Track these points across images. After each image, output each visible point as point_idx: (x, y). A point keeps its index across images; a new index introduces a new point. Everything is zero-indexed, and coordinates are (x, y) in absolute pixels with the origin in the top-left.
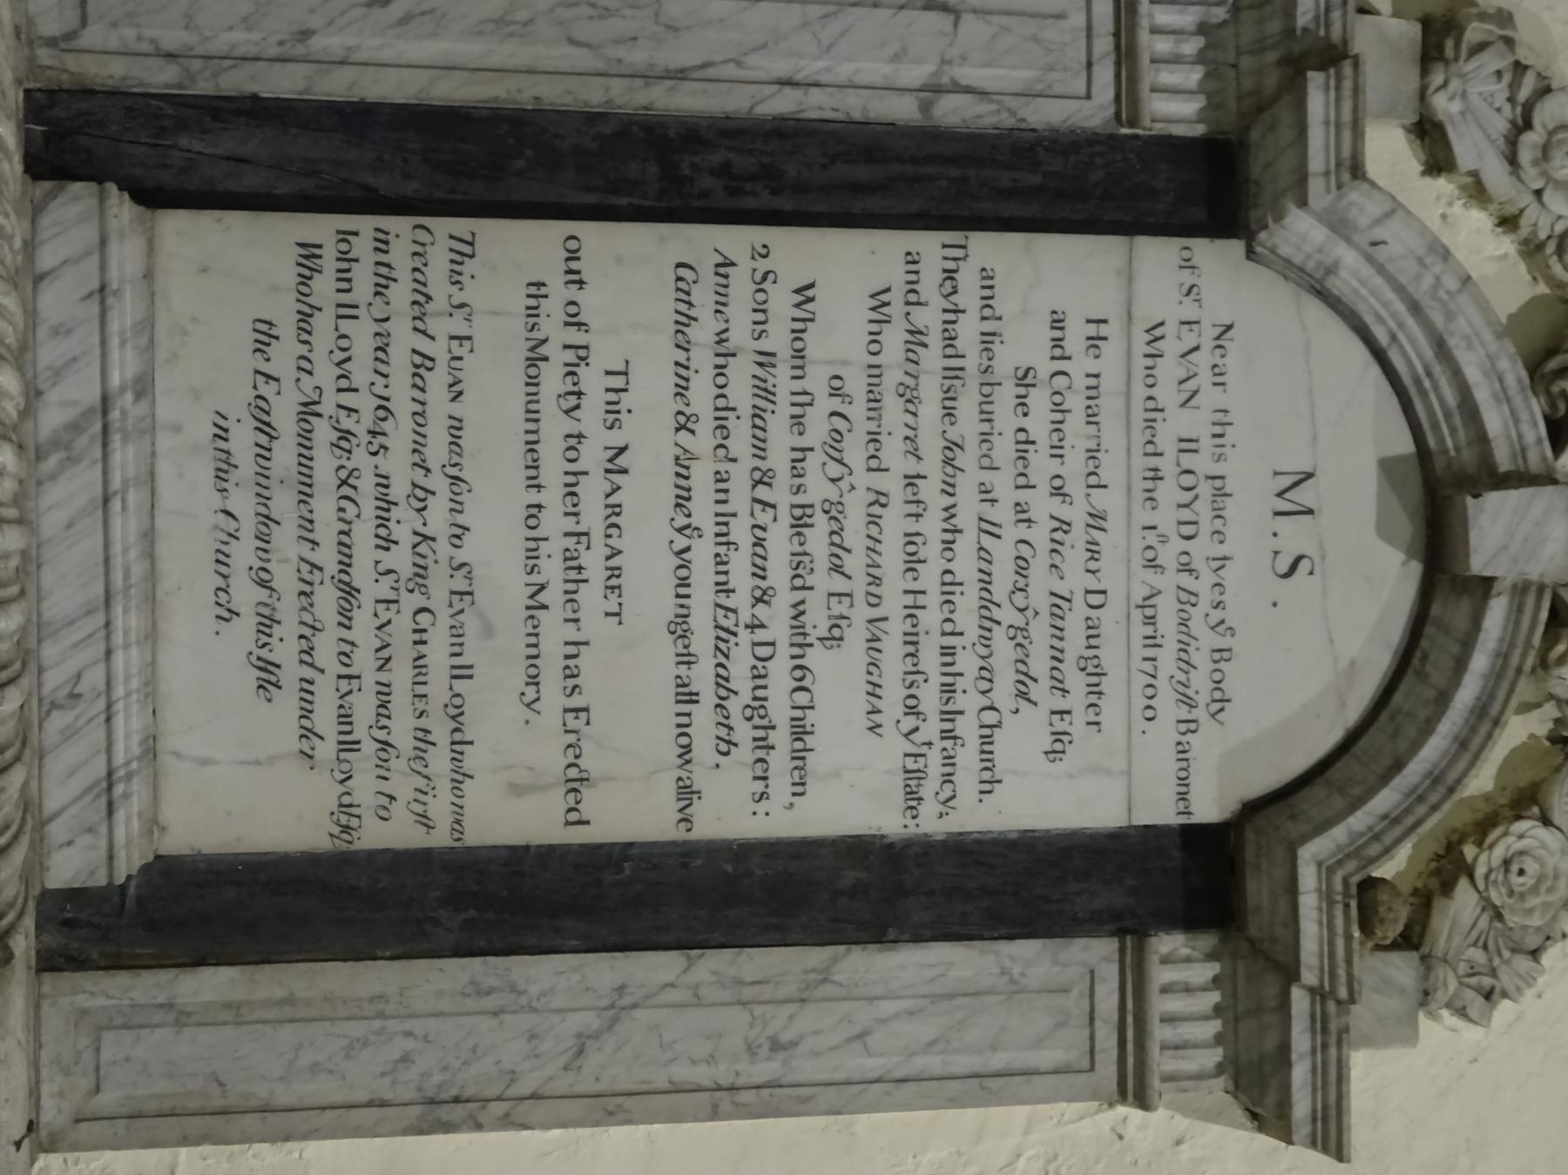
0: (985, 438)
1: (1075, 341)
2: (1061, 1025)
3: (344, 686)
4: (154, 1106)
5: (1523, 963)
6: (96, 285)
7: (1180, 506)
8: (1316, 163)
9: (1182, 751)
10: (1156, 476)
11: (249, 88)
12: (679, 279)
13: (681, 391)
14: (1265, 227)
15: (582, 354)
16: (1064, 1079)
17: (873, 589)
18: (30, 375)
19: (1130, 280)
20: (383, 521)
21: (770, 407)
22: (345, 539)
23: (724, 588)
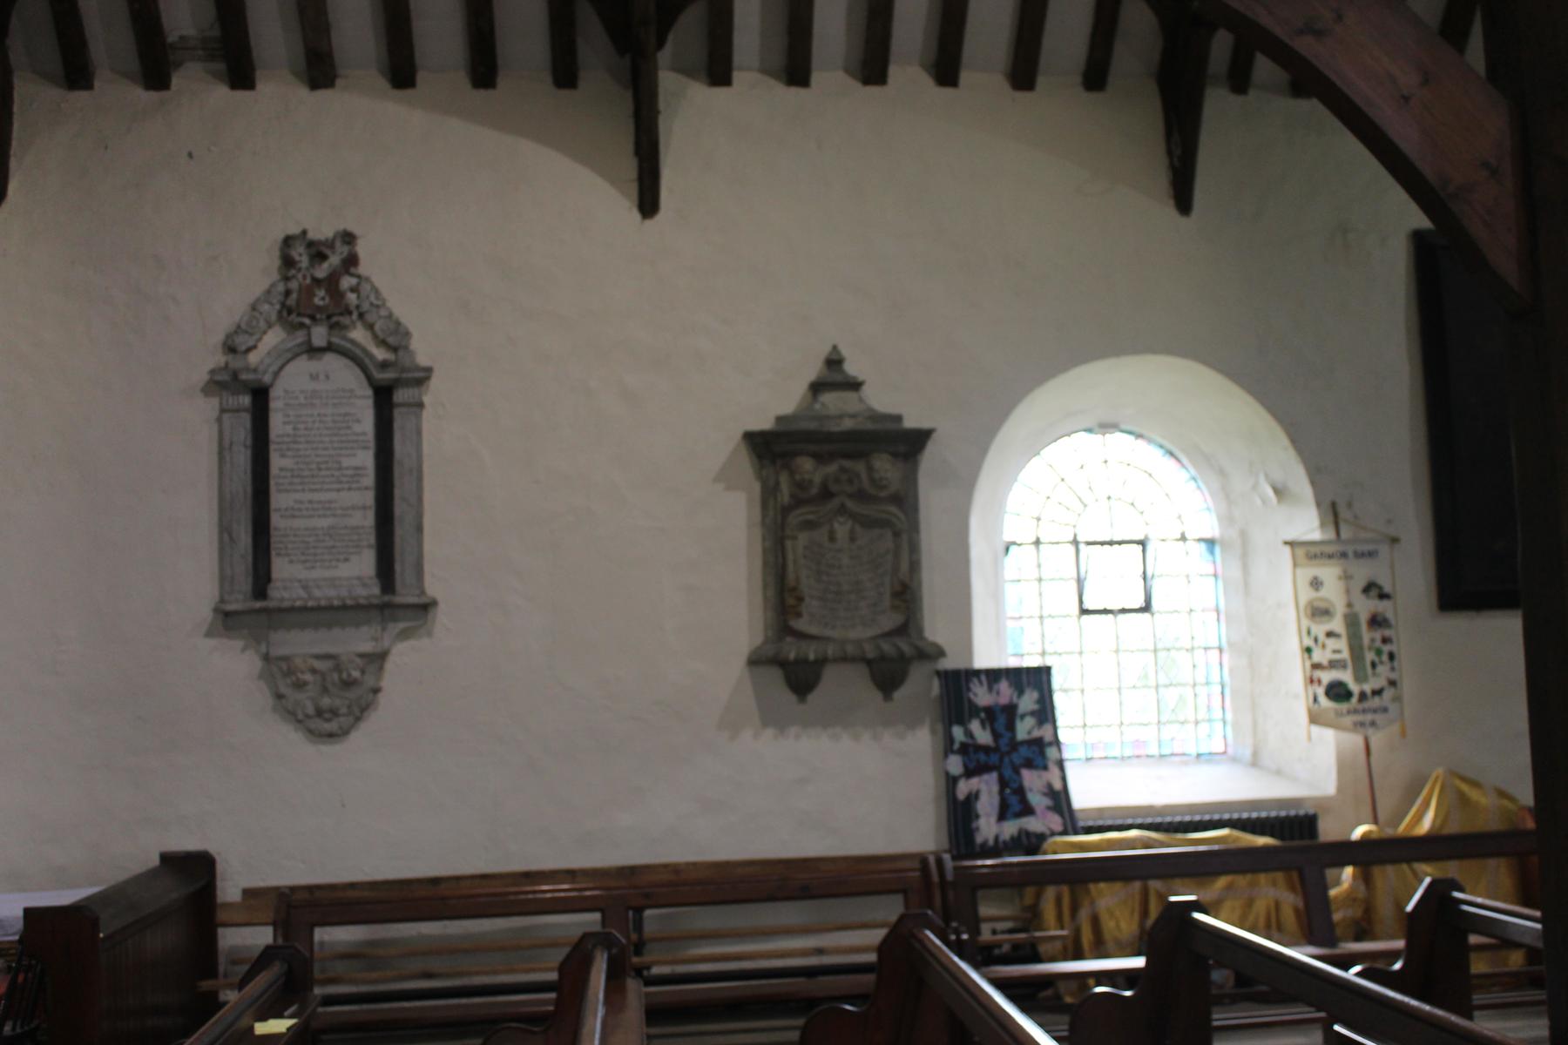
16: (419, 417)
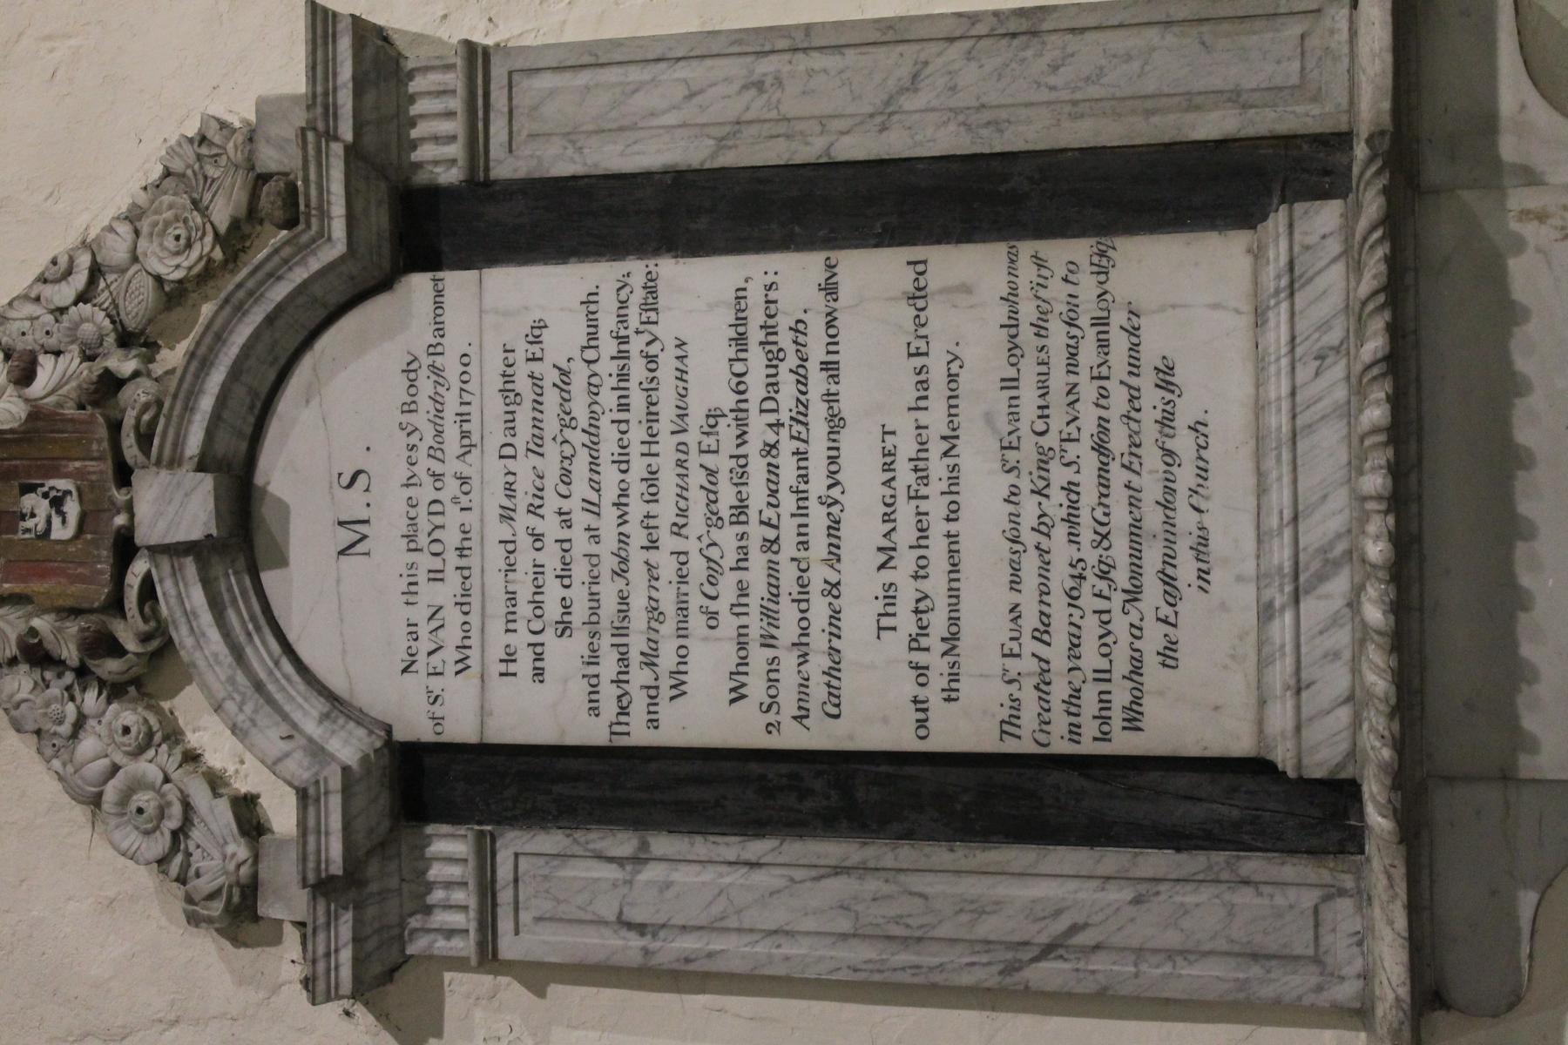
0: (595, 580)
2: (535, 108)
3: (1104, 371)
4: (1259, 24)
5: (178, 166)
6: (1304, 694)
7: (443, 527)
8: (335, 802)
9: (440, 330)
10: (461, 551)
11: (1183, 857)
12: (838, 706)
13: (835, 615)
14: (376, 751)
15: (915, 644)
16: (532, 64)
17: (683, 457)
18: (1357, 620)
19: (482, 707)
20: (1073, 505)
21: (765, 603)
22: (1104, 491)
23: (802, 456)
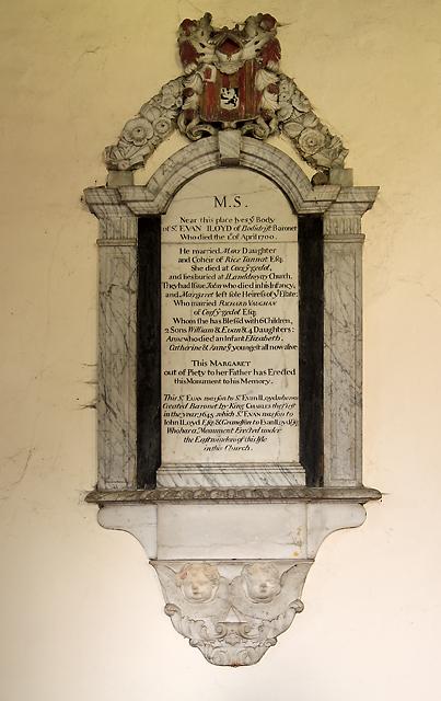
1: (185, 256)
5: (334, 141)
15: (190, 371)
